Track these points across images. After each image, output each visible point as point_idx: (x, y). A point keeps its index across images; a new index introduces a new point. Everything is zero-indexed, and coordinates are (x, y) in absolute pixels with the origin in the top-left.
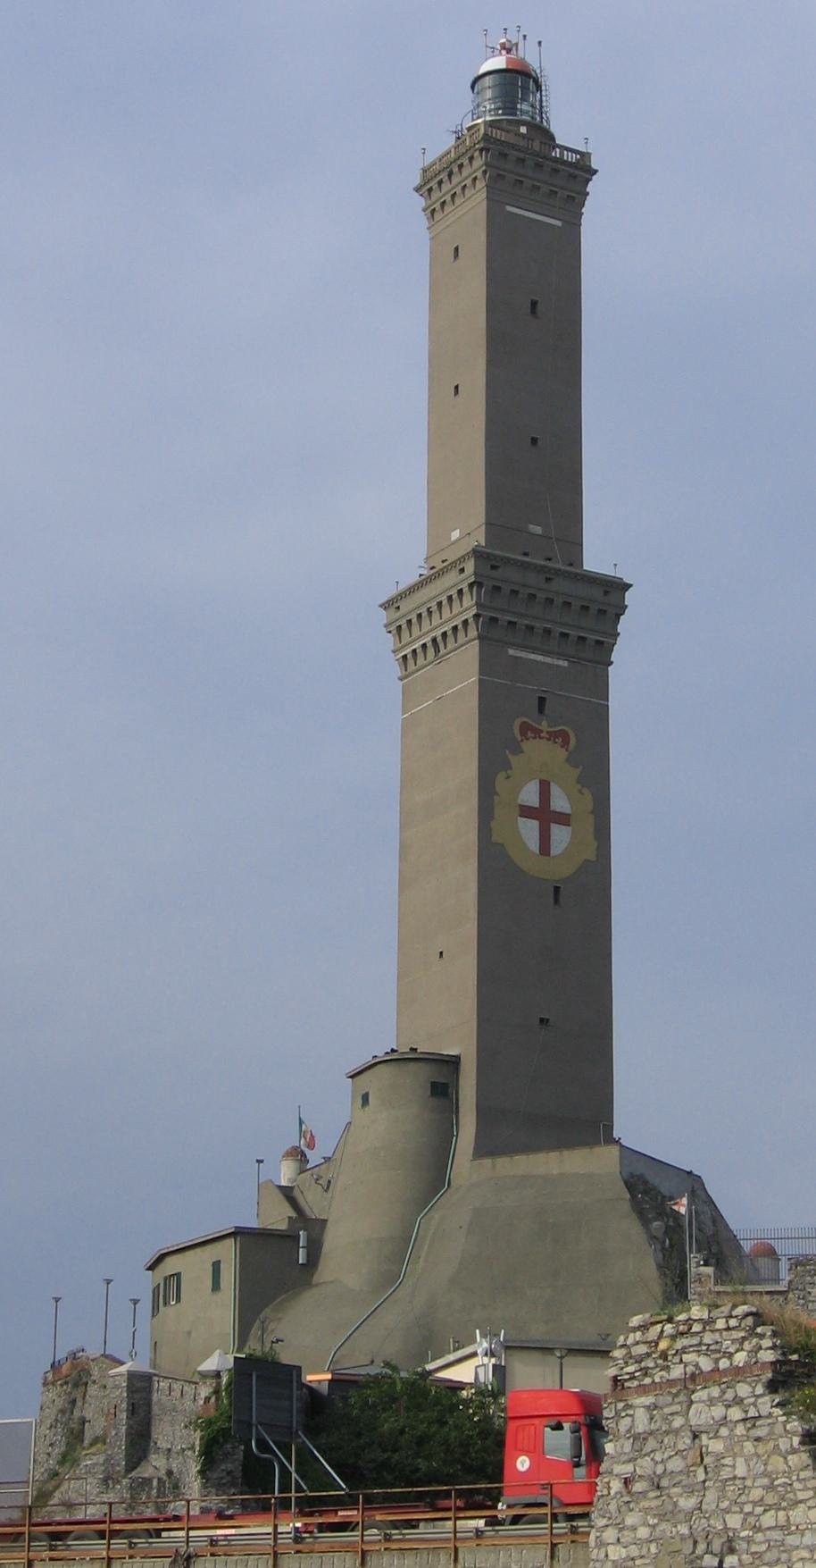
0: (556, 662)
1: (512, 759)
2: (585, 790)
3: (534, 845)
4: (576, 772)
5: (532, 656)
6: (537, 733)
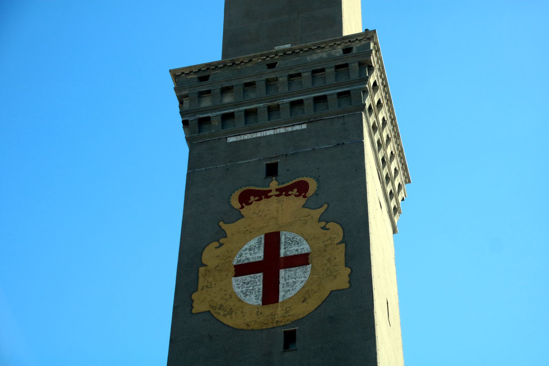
0: (290, 129)
1: (228, 228)
2: (329, 225)
3: (254, 299)
4: (317, 213)
5: (259, 135)
6: (263, 195)
